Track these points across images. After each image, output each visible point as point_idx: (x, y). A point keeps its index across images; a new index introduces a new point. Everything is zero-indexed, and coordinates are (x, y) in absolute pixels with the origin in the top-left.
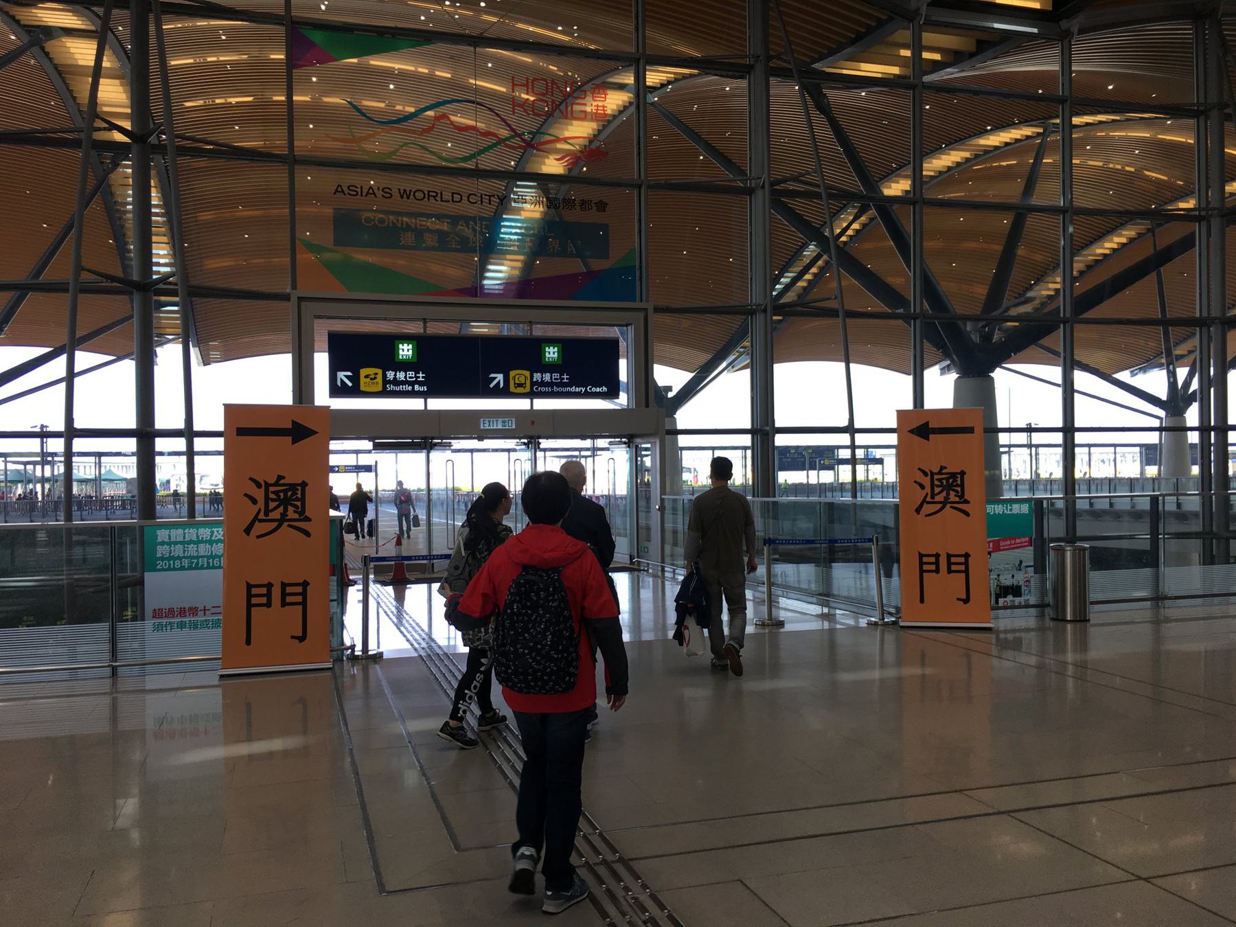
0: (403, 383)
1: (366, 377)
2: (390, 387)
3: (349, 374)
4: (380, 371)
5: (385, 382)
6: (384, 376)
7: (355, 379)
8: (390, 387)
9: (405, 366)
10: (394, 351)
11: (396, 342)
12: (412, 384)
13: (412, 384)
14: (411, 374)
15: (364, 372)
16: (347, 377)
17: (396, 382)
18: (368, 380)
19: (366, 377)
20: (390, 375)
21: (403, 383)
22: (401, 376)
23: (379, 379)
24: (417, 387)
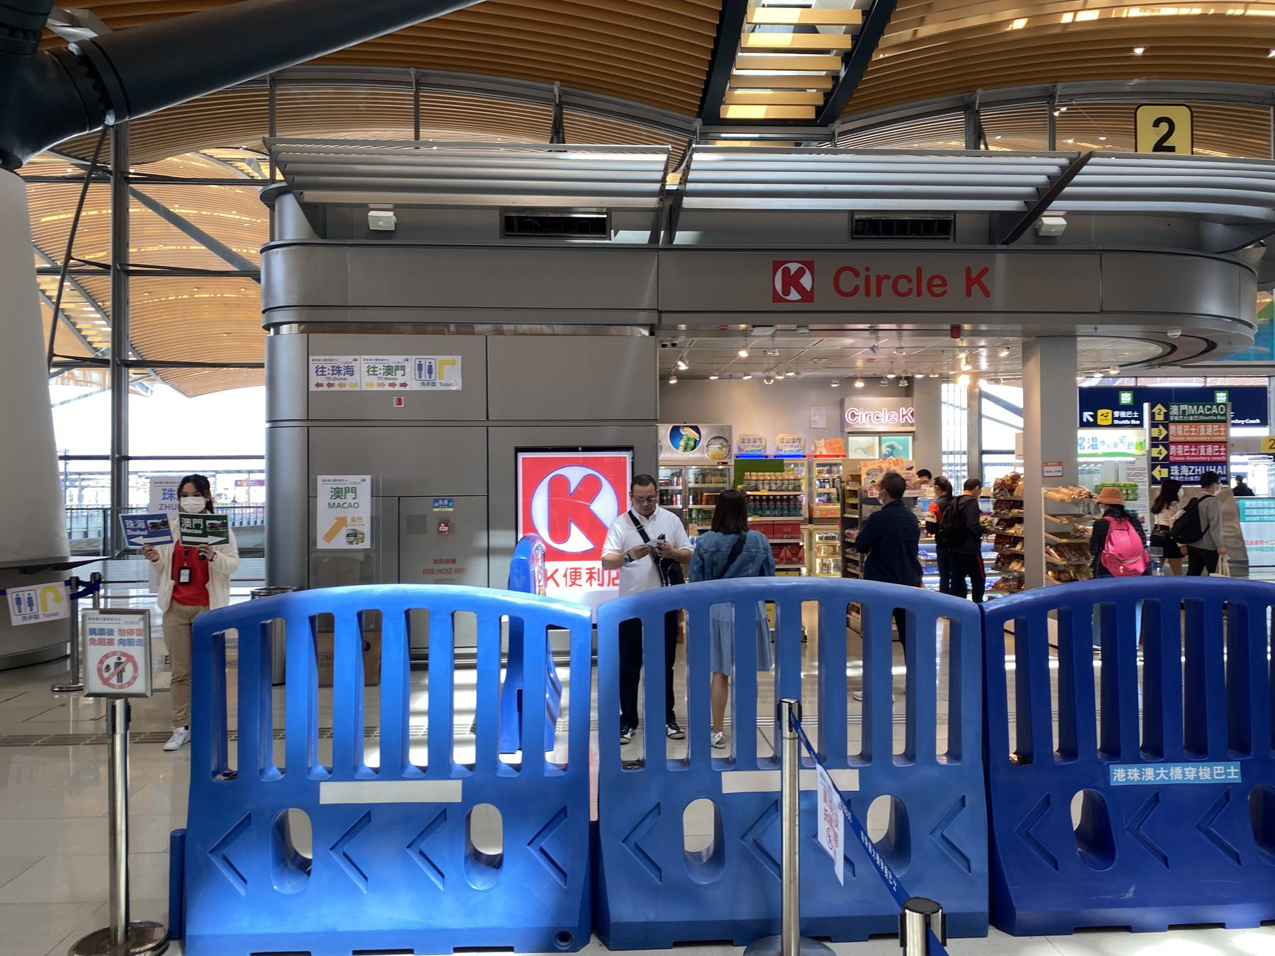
0: (1125, 419)
1: (1102, 415)
2: (1116, 422)
3: (1092, 413)
4: (1110, 411)
5: (1114, 418)
6: (1113, 415)
7: (1094, 417)
8: (1116, 422)
9: (1125, 408)
10: (1118, 398)
11: (1120, 392)
12: (1130, 419)
13: (1130, 419)
14: (1130, 413)
15: (1100, 412)
16: (1091, 416)
17: (1120, 419)
18: (1103, 417)
19: (1102, 415)
20: (1117, 414)
21: (1125, 419)
22: (1123, 414)
23: (1110, 416)
24: (1133, 422)
